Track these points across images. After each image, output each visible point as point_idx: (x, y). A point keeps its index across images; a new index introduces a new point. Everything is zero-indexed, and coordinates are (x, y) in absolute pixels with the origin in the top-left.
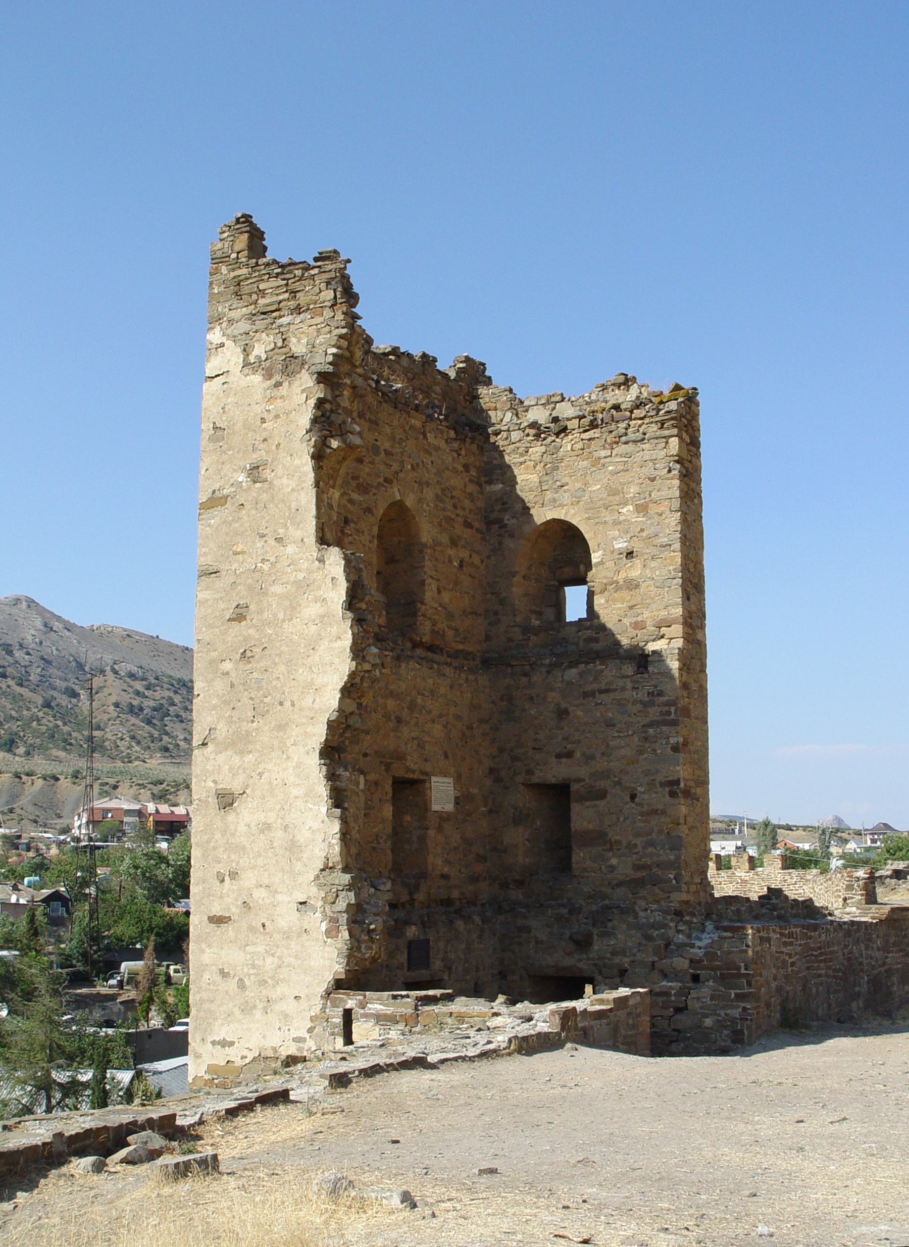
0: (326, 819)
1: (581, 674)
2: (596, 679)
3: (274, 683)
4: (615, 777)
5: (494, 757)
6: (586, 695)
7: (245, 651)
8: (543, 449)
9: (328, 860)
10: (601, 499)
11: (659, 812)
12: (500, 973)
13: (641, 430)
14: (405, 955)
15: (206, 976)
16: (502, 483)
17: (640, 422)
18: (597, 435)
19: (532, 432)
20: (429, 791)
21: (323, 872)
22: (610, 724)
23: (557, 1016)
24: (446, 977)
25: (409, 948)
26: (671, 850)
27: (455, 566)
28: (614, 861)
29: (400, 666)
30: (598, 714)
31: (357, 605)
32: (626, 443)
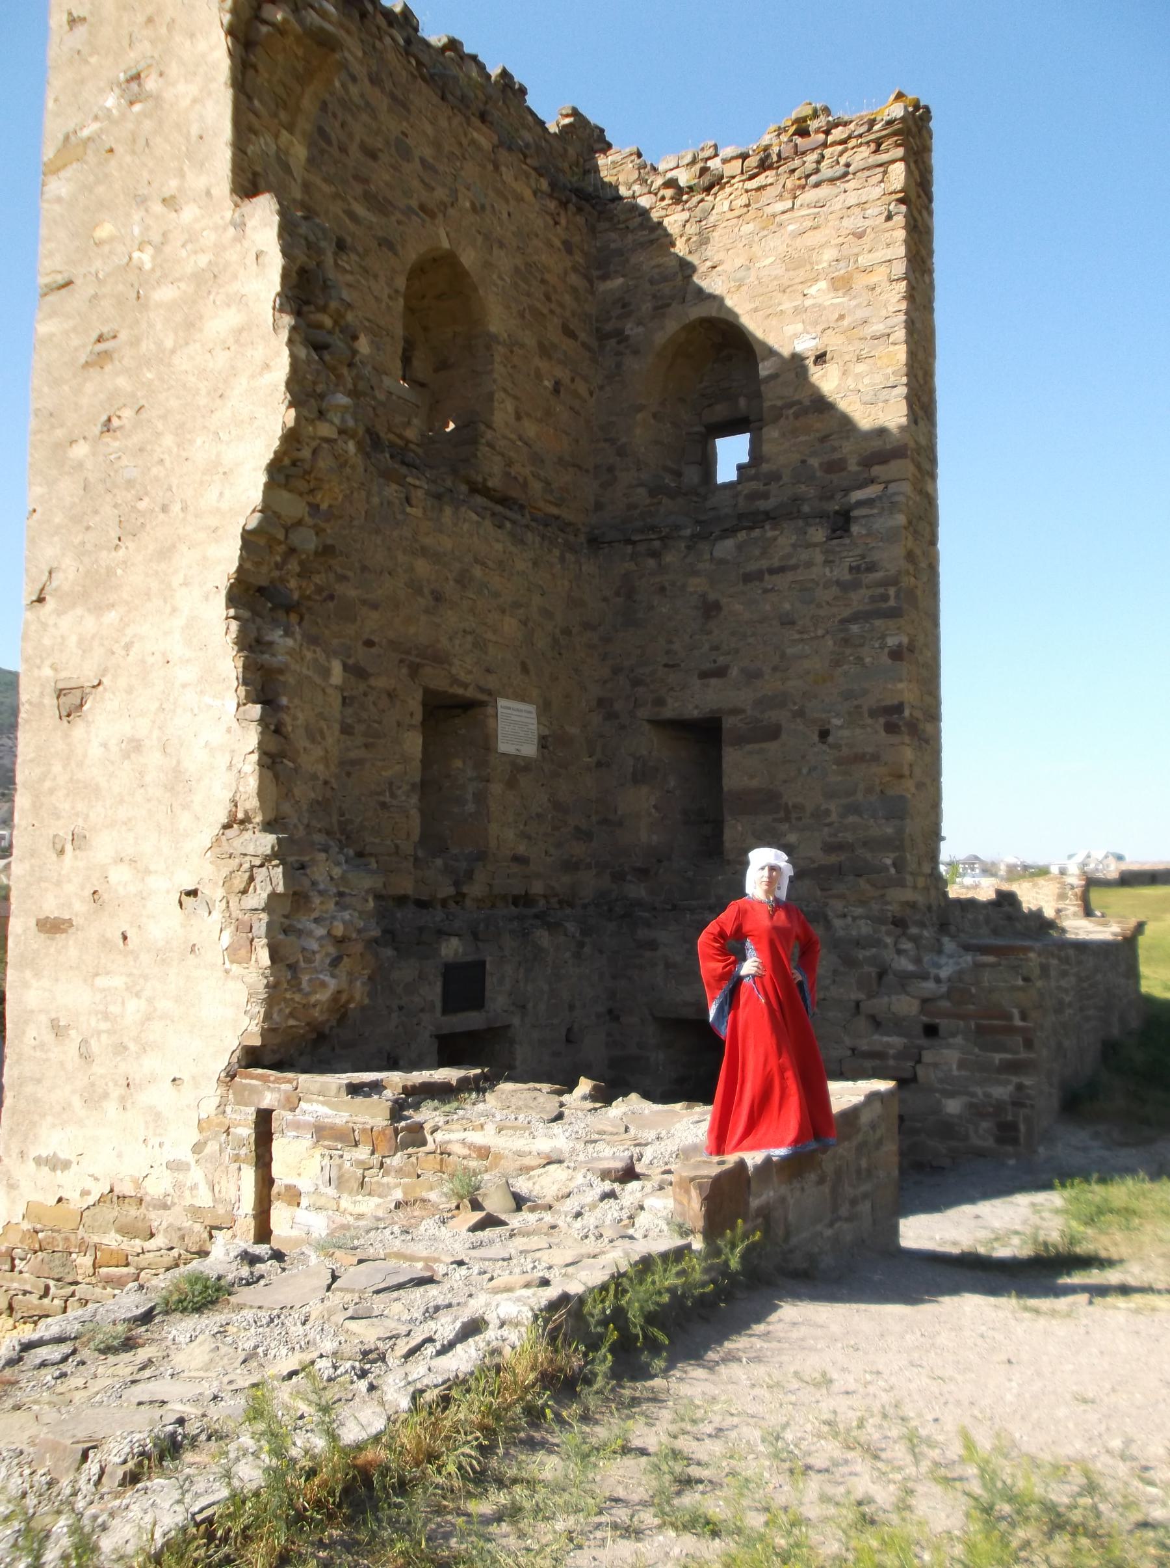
0: (235, 724)
1: (739, 547)
3: (154, 471)
4: (795, 704)
5: (605, 682)
6: (748, 578)
7: (109, 420)
8: (686, 215)
9: (236, 806)
10: (776, 278)
11: (868, 757)
12: (610, 1012)
13: (843, 160)
14: (438, 988)
15: (31, 1032)
16: (623, 276)
17: (840, 148)
18: (770, 180)
19: (669, 193)
20: (491, 721)
21: (227, 832)
22: (788, 621)
23: (694, 1193)
24: (516, 1021)
26: (887, 819)
27: (546, 388)
29: (441, 510)
30: (768, 607)
31: (312, 316)
32: (817, 185)
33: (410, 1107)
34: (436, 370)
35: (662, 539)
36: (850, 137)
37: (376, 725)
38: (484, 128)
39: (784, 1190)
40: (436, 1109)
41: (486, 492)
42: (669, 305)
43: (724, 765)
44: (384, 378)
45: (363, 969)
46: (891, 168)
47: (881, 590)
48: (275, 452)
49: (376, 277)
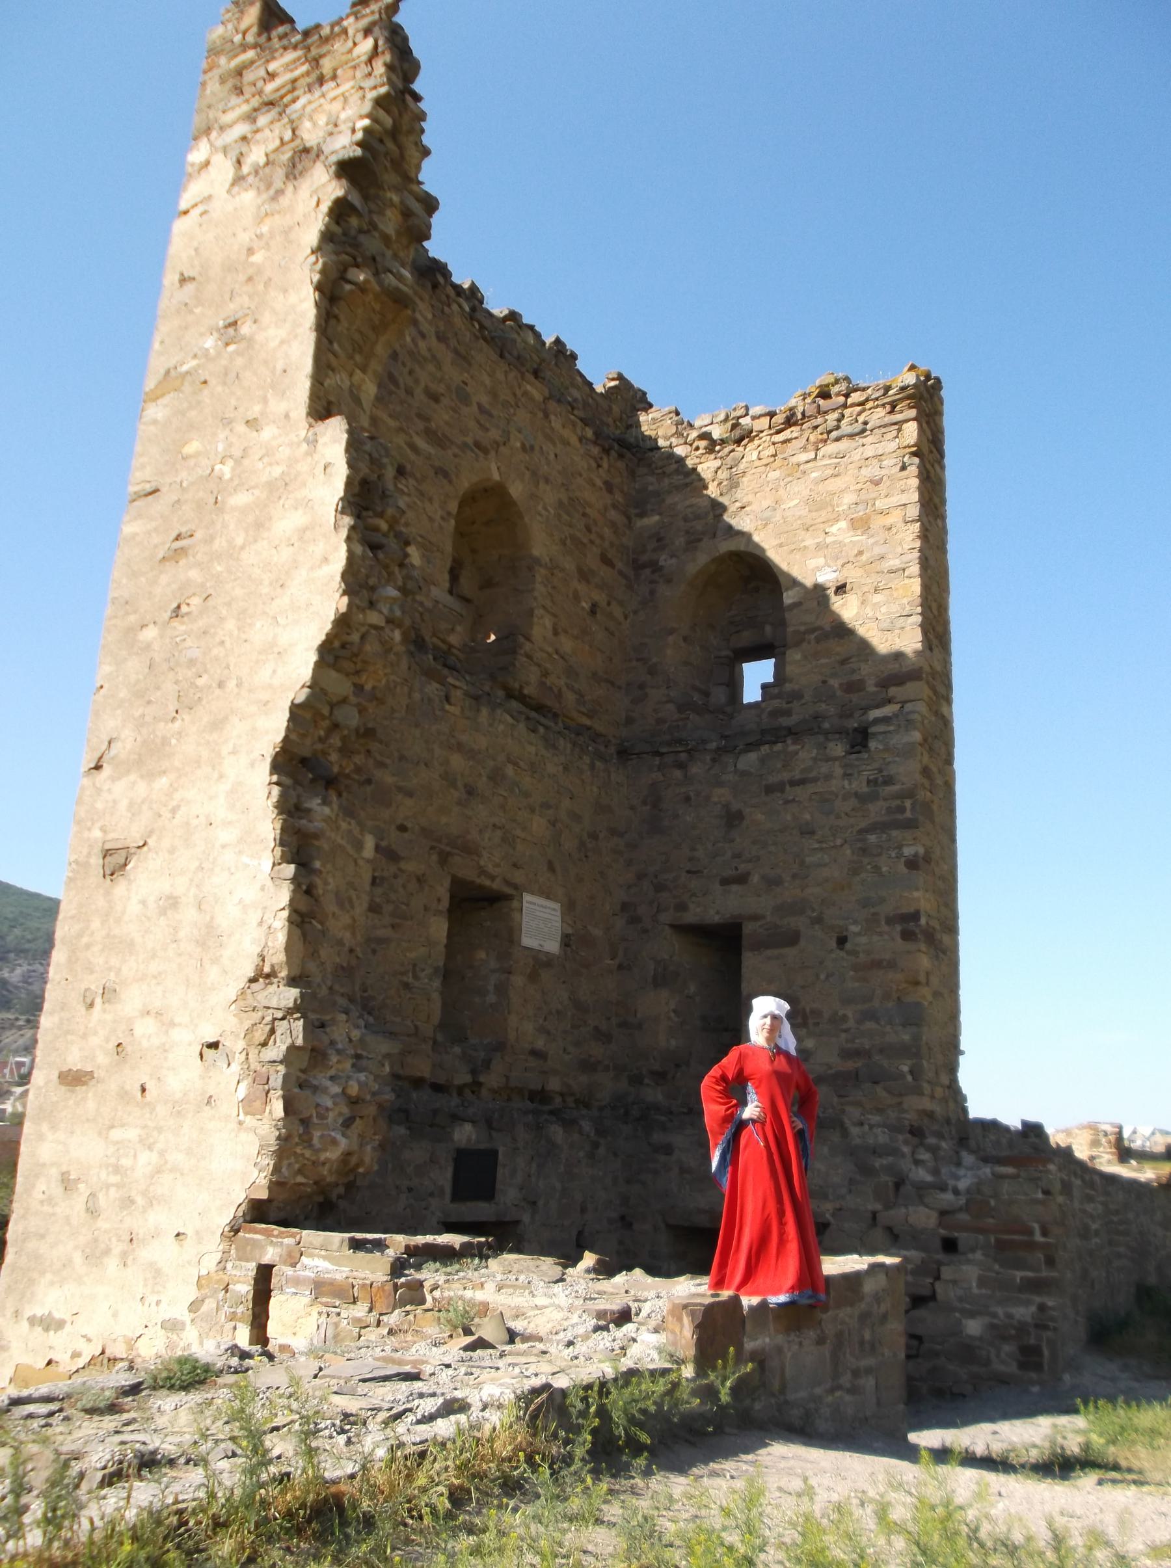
0: (269, 883)
1: (762, 761)
3: (215, 651)
4: (813, 910)
5: (629, 887)
6: (769, 789)
7: (179, 607)
8: (718, 463)
9: (263, 960)
10: (799, 518)
11: (885, 963)
12: (623, 1218)
13: (861, 419)
14: (449, 1173)
15: (41, 1186)
16: (660, 514)
17: (859, 408)
18: (795, 435)
19: (703, 444)
20: (516, 915)
21: (253, 985)
22: (807, 831)
23: (686, 1321)
24: (526, 1218)
27: (583, 608)
29: (478, 710)
30: (789, 818)
31: (370, 521)
32: (838, 439)
33: (411, 1266)
34: (481, 588)
35: (689, 752)
36: (867, 400)
37: (404, 907)
38: (536, 382)
39: (780, 1339)
40: (437, 1271)
41: (522, 699)
42: (700, 540)
43: (744, 970)
44: (432, 588)
45: (375, 1134)
46: (905, 426)
47: (898, 802)
48: (327, 635)
49: (430, 500)
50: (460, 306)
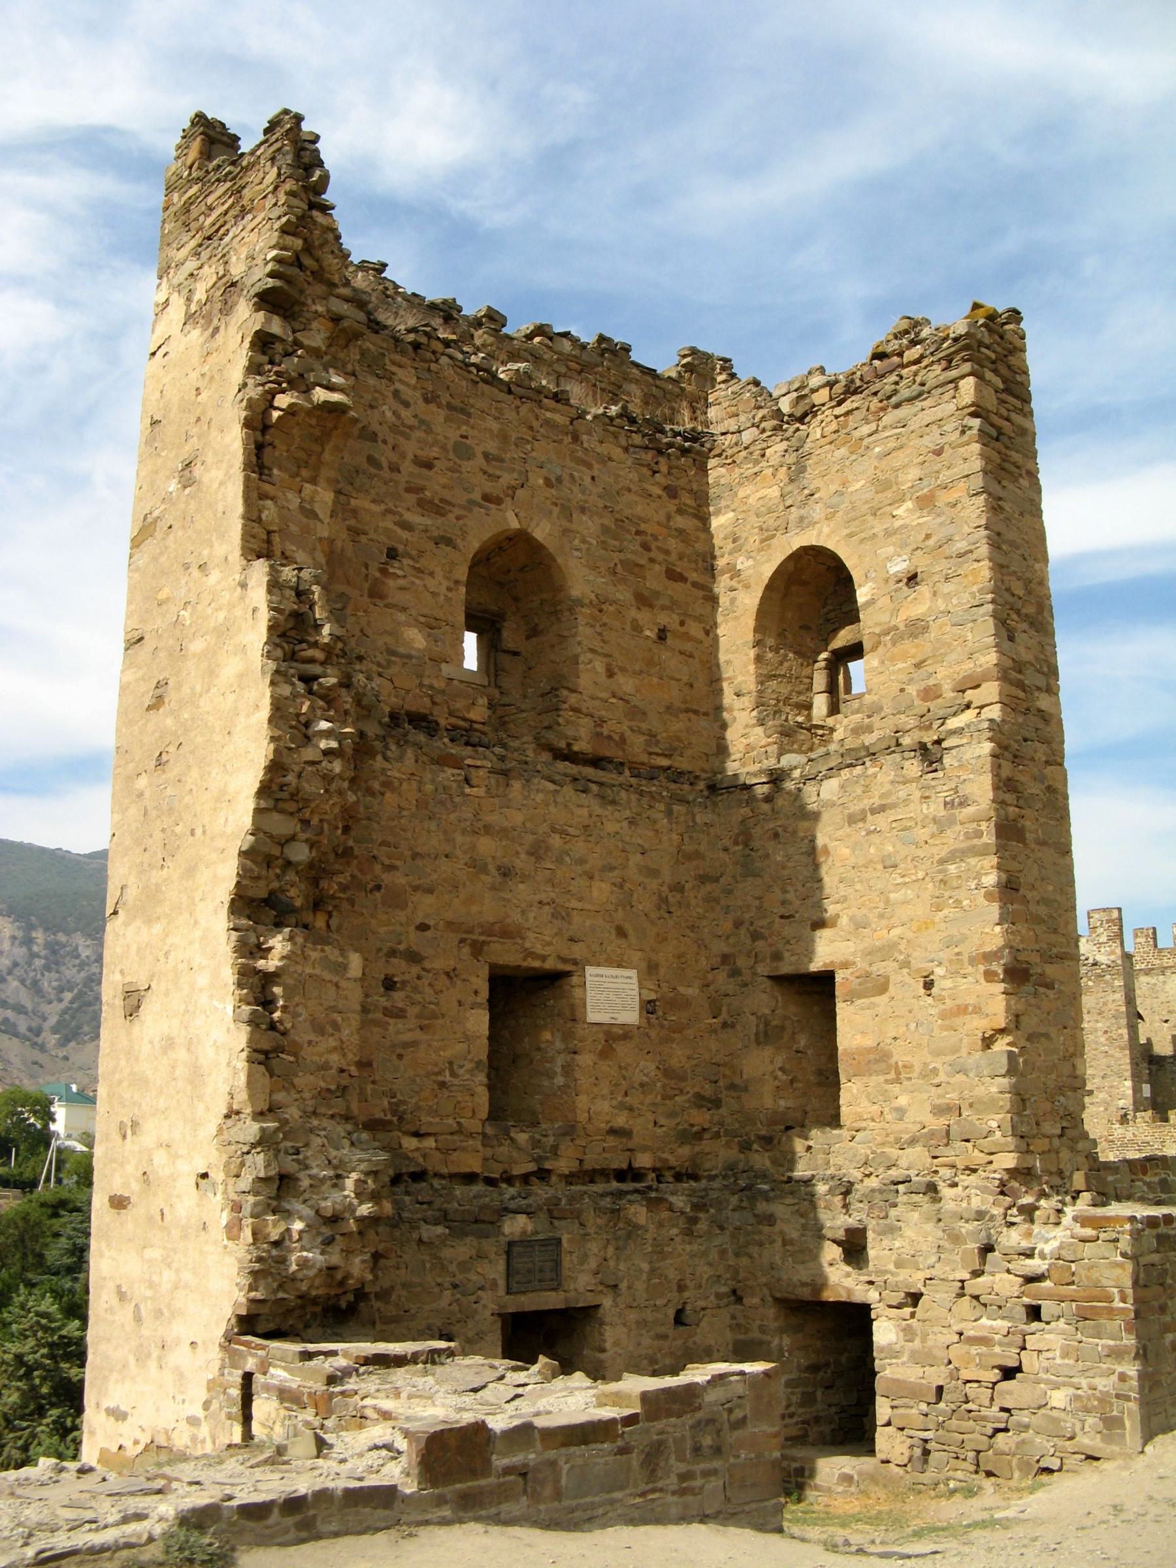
0: (232, 1026)
2: (867, 789)
6: (852, 820)
7: (161, 754)
10: (866, 502)
11: (970, 1009)
12: (734, 1292)
13: (918, 379)
14: (501, 1266)
15: (105, 1297)
16: (733, 511)
17: (914, 368)
18: (855, 405)
20: (577, 992)
22: (890, 865)
25: (508, 1253)
28: (903, 1101)
32: (897, 406)
34: (528, 638)
36: (922, 357)
37: (432, 1006)
38: (559, 406)
41: (570, 756)
42: (774, 536)
44: (444, 665)
46: (962, 383)
47: (974, 825)
48: (261, 782)
49: (432, 574)
50: (451, 358)
